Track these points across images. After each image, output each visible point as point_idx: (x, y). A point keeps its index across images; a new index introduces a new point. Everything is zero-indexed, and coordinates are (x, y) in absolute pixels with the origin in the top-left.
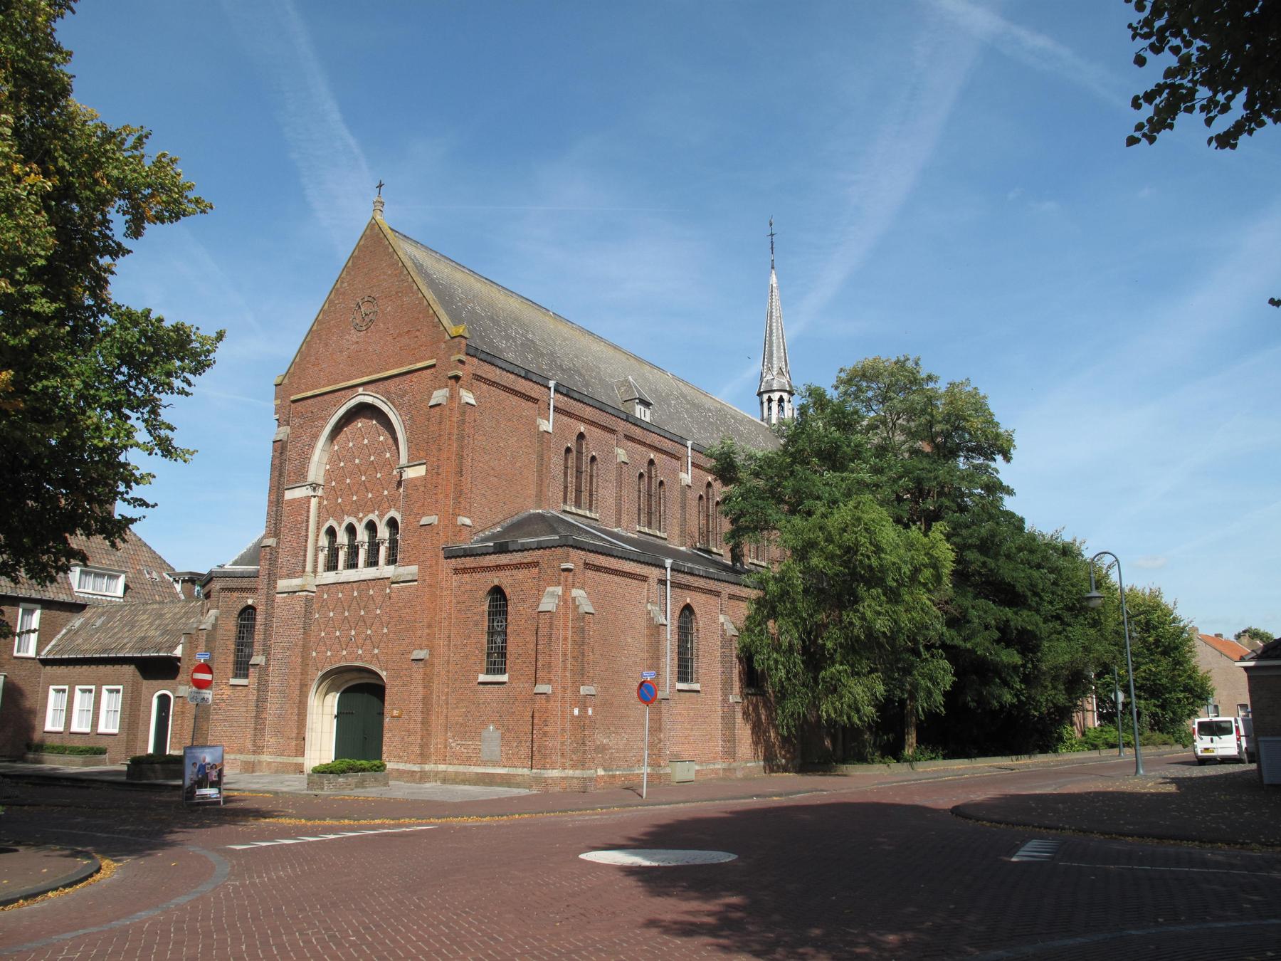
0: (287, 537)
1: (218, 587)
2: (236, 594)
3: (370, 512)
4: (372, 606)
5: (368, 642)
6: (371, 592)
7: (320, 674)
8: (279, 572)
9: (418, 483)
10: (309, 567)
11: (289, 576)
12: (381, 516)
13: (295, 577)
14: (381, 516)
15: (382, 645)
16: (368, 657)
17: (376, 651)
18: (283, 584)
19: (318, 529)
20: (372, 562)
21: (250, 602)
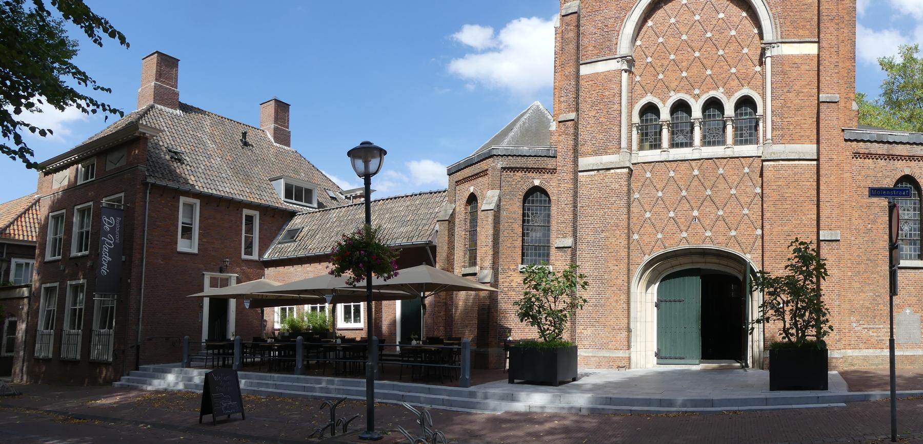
0: (589, 114)
1: (499, 166)
2: (519, 174)
3: (709, 89)
4: (722, 185)
5: (720, 223)
6: (721, 171)
7: (647, 258)
8: (582, 149)
9: (797, 61)
10: (624, 144)
11: (596, 153)
12: (729, 94)
13: (606, 153)
14: (729, 94)
15: (742, 226)
16: (721, 239)
17: (733, 233)
18: (585, 162)
19: (631, 105)
20: (713, 138)
21: (537, 183)
